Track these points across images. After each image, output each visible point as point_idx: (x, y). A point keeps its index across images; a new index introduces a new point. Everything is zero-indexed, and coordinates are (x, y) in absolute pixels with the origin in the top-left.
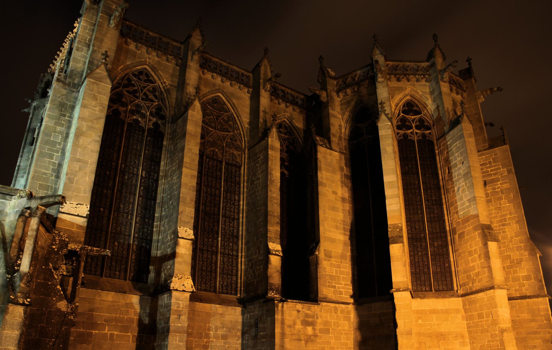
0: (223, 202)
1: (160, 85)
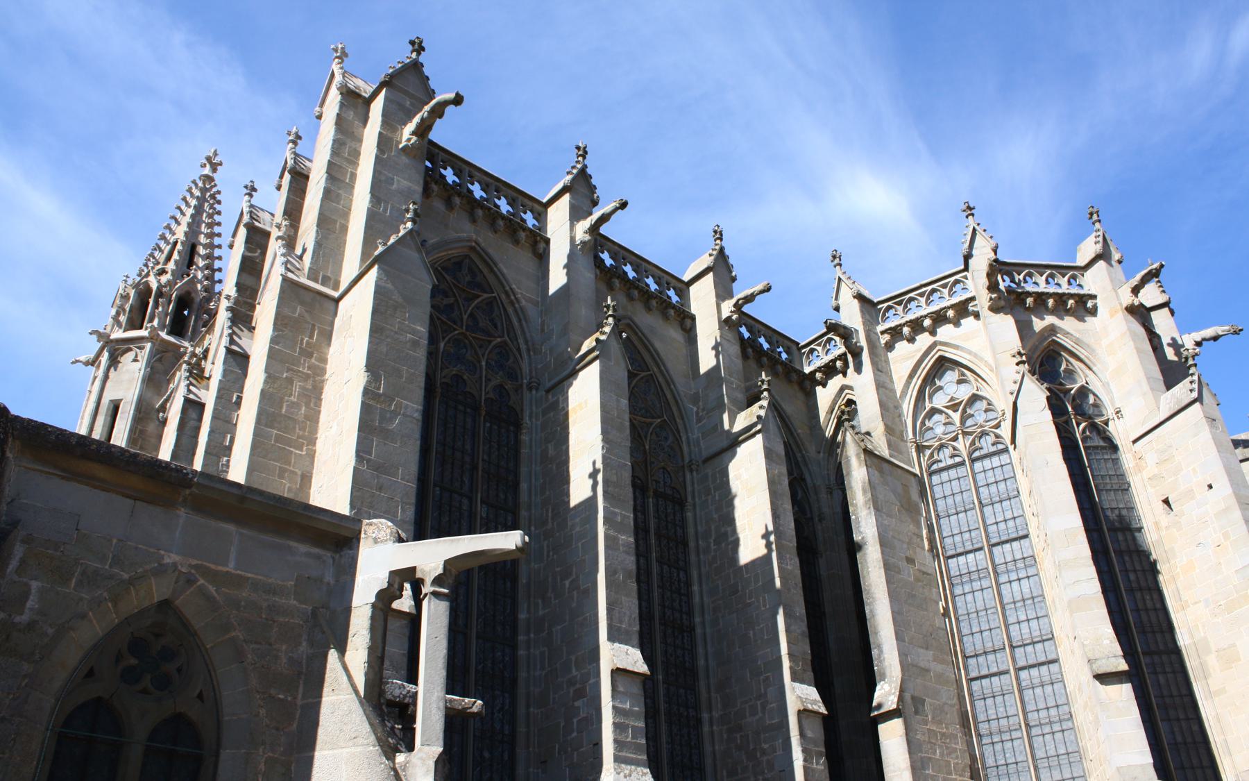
1: (503, 297)
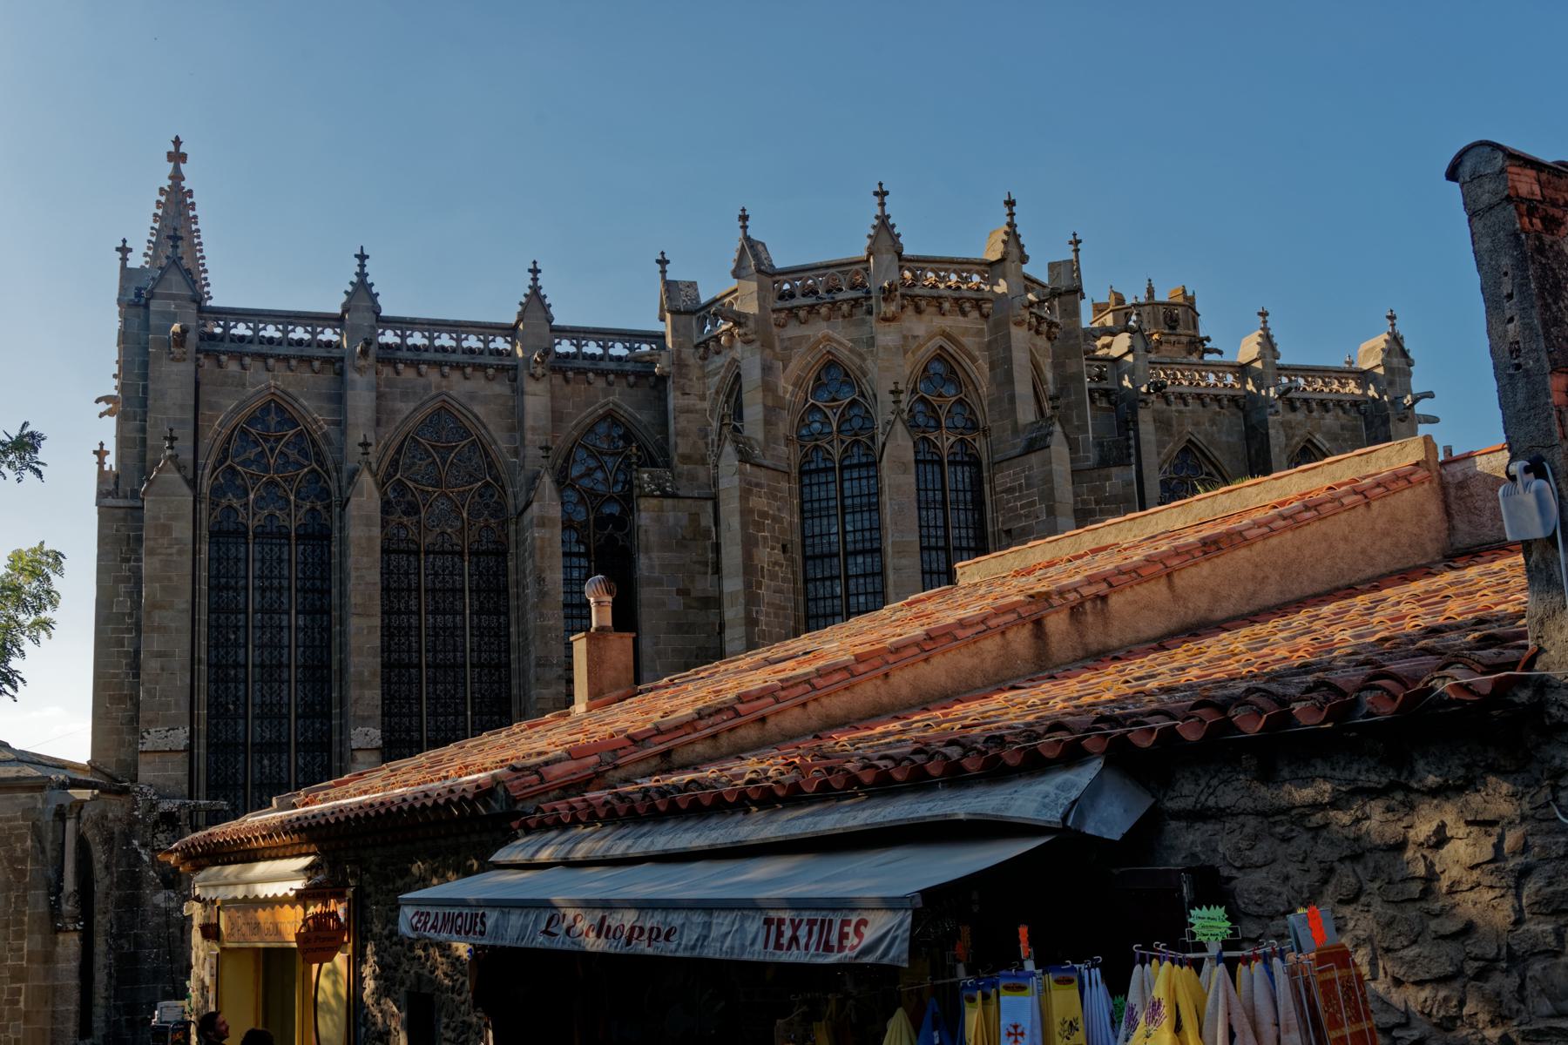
0: (472, 635)
